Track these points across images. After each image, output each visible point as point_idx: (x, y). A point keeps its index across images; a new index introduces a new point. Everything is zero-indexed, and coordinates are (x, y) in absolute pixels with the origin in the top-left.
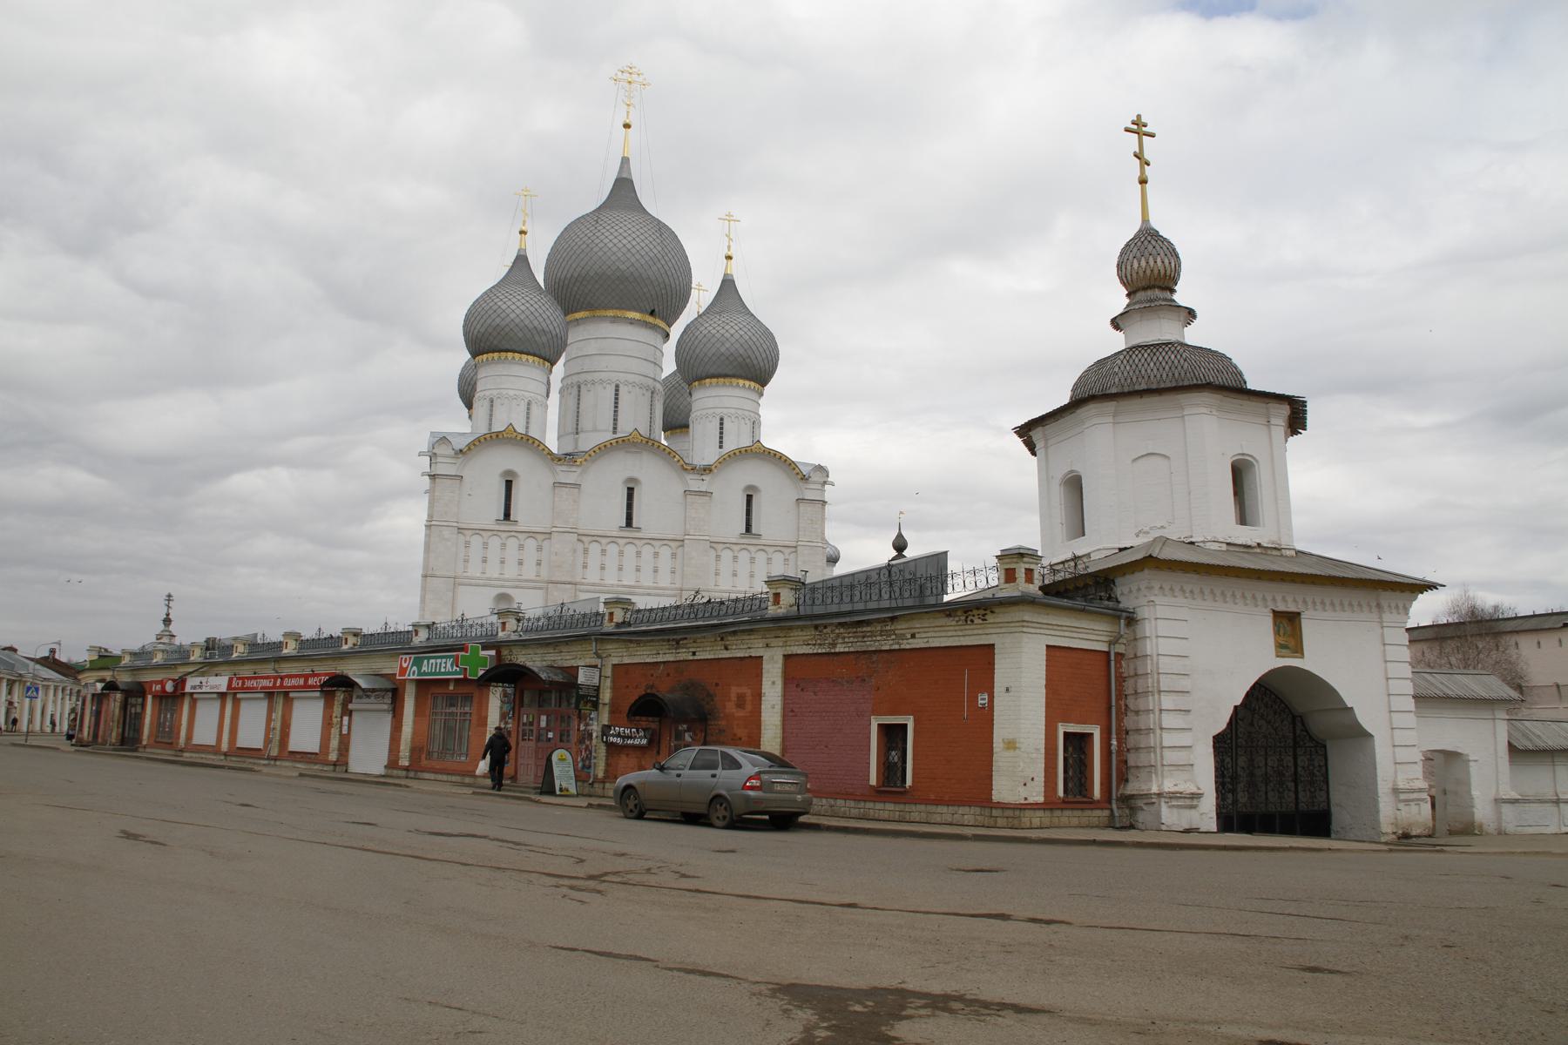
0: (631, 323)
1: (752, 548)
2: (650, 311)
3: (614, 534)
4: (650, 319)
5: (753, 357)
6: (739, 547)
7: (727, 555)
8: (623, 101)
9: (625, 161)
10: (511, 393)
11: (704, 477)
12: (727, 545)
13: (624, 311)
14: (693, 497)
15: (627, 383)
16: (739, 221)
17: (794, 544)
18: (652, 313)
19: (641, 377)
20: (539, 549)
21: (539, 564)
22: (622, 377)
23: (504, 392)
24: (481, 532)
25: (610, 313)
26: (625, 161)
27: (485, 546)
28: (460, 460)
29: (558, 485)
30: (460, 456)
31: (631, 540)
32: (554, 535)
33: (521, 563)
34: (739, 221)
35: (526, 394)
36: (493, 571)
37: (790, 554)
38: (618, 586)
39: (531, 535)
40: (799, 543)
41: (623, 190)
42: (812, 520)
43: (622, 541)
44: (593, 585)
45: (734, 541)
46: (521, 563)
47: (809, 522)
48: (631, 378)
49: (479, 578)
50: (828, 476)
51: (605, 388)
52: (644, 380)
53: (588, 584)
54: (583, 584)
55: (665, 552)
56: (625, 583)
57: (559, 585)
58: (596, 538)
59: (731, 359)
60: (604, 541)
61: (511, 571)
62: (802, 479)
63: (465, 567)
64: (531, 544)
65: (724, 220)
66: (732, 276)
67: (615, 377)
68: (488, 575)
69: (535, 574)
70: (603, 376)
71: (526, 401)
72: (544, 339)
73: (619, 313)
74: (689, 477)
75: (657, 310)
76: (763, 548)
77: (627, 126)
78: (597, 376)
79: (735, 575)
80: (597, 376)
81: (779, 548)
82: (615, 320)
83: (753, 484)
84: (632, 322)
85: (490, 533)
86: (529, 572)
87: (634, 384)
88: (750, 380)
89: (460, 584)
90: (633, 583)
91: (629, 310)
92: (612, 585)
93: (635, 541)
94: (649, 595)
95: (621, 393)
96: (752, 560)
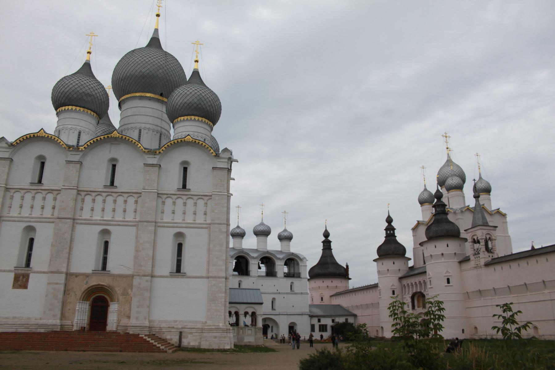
0: (150, 100)
1: (184, 197)
2: (160, 93)
3: (100, 190)
4: (160, 98)
5: (202, 104)
6: (176, 197)
7: (169, 202)
8: (157, 5)
9: (156, 31)
10: (70, 126)
11: (156, 156)
12: (169, 196)
13: (145, 93)
14: (149, 167)
15: (145, 128)
16: (202, 44)
17: (210, 194)
18: (161, 95)
19: (154, 126)
20: (55, 199)
21: (54, 208)
22: (143, 126)
23: (66, 126)
24: (21, 190)
25: (138, 94)
26: (156, 31)
27: (23, 198)
28: (11, 150)
29: (69, 162)
30: (12, 147)
31: (110, 193)
32: (63, 192)
33: (43, 208)
34: (202, 44)
35: (79, 128)
36: (26, 213)
37: (208, 200)
38: (100, 220)
39: (50, 191)
40: (213, 193)
41: (155, 42)
42: (221, 180)
43: (104, 194)
44: (85, 220)
45: (173, 192)
46: (43, 208)
47: (220, 181)
48: (148, 126)
49: (15, 217)
50: (231, 154)
51: (134, 131)
52: (155, 128)
53: (82, 220)
54: (79, 219)
55: (131, 200)
56: (105, 218)
57: (63, 220)
58: (88, 193)
59: (190, 105)
60: (94, 194)
61: (37, 213)
62: (216, 156)
63: (9, 211)
64: (50, 197)
65: (195, 44)
66: (198, 69)
67: (139, 125)
68: (22, 215)
69: (51, 214)
70: (133, 125)
71: (78, 131)
72: (89, 99)
73: (143, 94)
74: (146, 156)
75: (164, 93)
76: (191, 197)
77: (158, 15)
78: (130, 126)
79: (173, 213)
80: (130, 126)
81: (201, 197)
82: (141, 98)
83: (187, 160)
84: (150, 99)
85: (26, 191)
86: (48, 213)
87: (149, 129)
88: (202, 117)
89: (3, 221)
90: (110, 219)
91: (149, 93)
92: (96, 220)
93: (113, 194)
94: (119, 225)
95: (142, 133)
96: (185, 204)
